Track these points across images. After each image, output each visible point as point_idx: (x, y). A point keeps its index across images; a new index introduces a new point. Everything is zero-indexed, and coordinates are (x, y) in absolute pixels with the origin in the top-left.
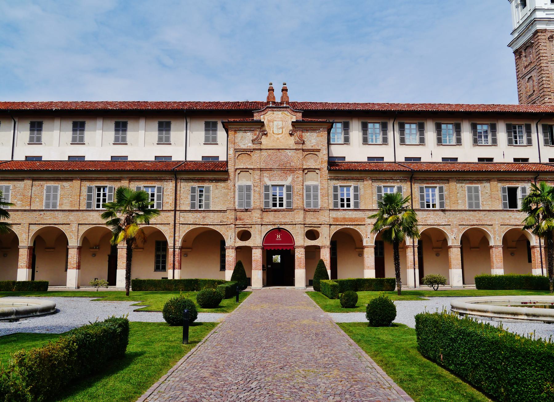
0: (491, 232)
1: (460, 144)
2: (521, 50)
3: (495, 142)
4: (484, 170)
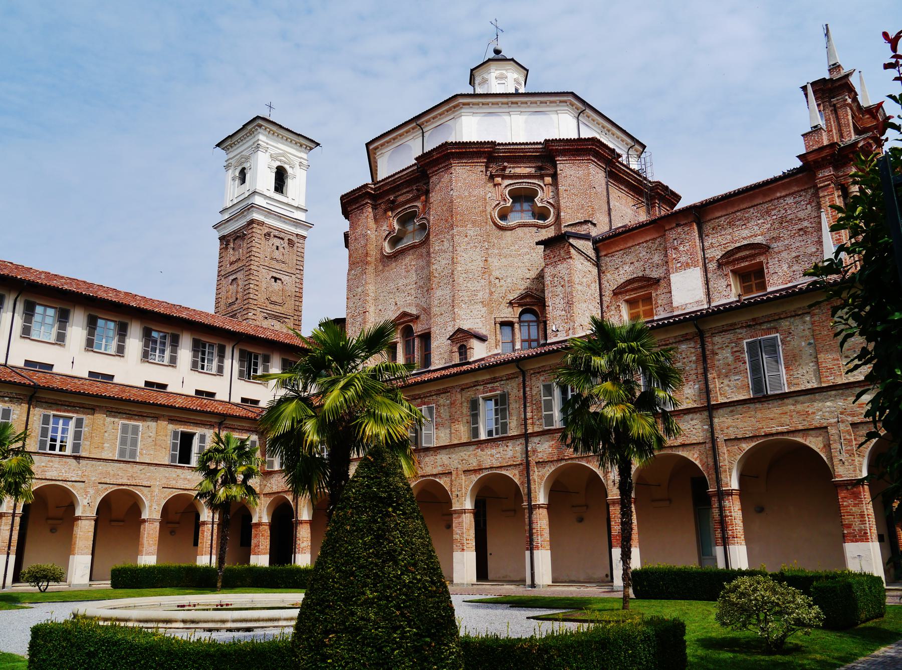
0: (146, 497)
1: (121, 355)
2: (229, 238)
3: (173, 361)
4: (151, 402)
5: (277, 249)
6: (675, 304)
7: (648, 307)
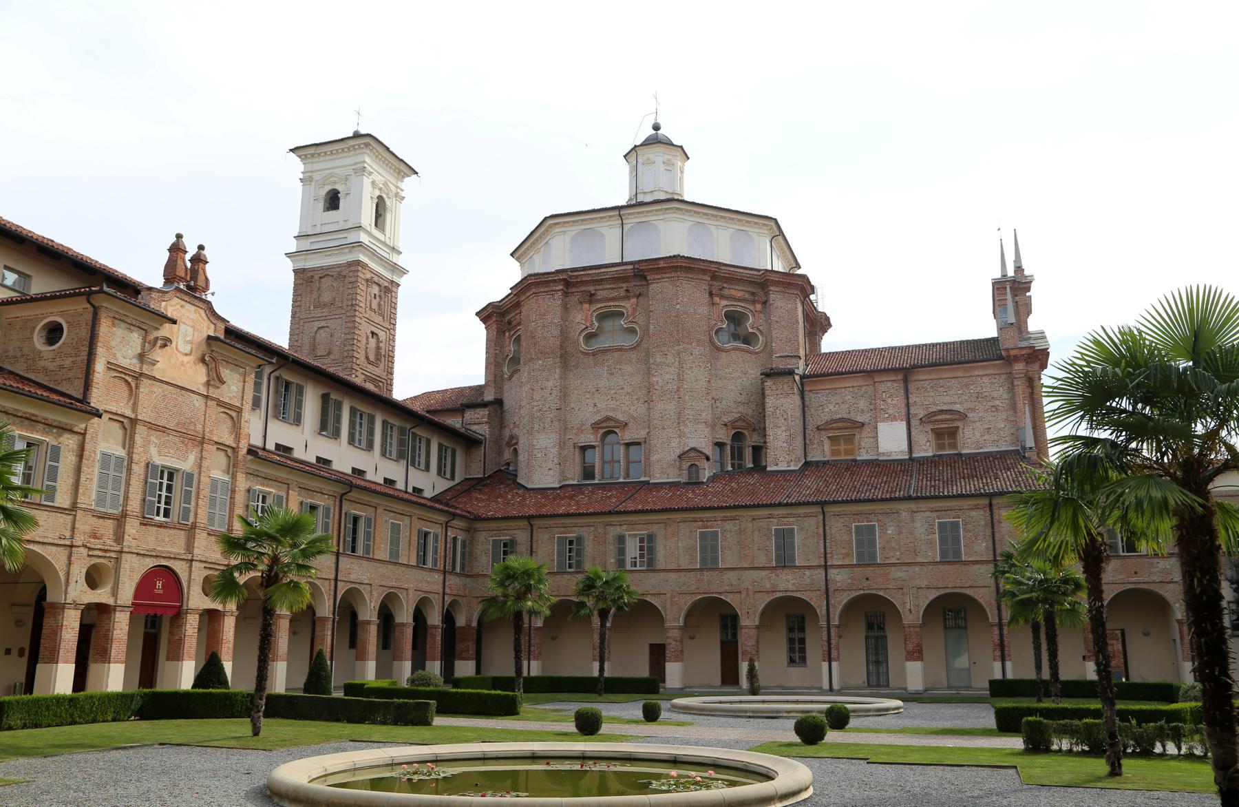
6: (881, 450)
7: (849, 447)
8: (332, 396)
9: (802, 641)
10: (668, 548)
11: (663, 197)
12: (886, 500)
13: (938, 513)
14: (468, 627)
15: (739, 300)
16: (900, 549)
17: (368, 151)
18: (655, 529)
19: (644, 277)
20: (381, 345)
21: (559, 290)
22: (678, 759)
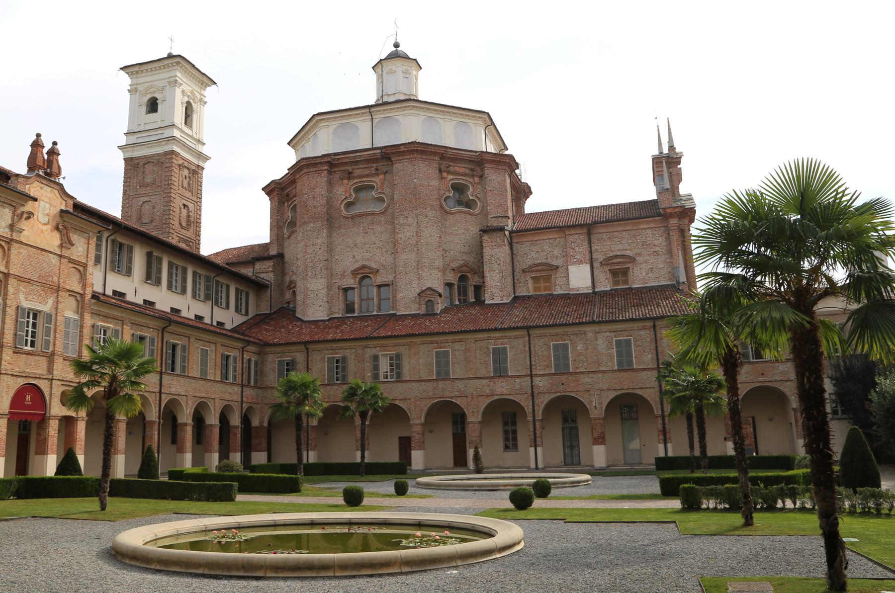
5: (186, 178)
6: (571, 286)
8: (154, 254)
9: (515, 432)
10: (411, 364)
11: (402, 98)
12: (576, 324)
13: (615, 333)
14: (261, 426)
15: (462, 175)
16: (587, 361)
17: (179, 68)
18: (401, 350)
19: (389, 159)
20: (191, 214)
21: (325, 170)
22: (422, 523)
